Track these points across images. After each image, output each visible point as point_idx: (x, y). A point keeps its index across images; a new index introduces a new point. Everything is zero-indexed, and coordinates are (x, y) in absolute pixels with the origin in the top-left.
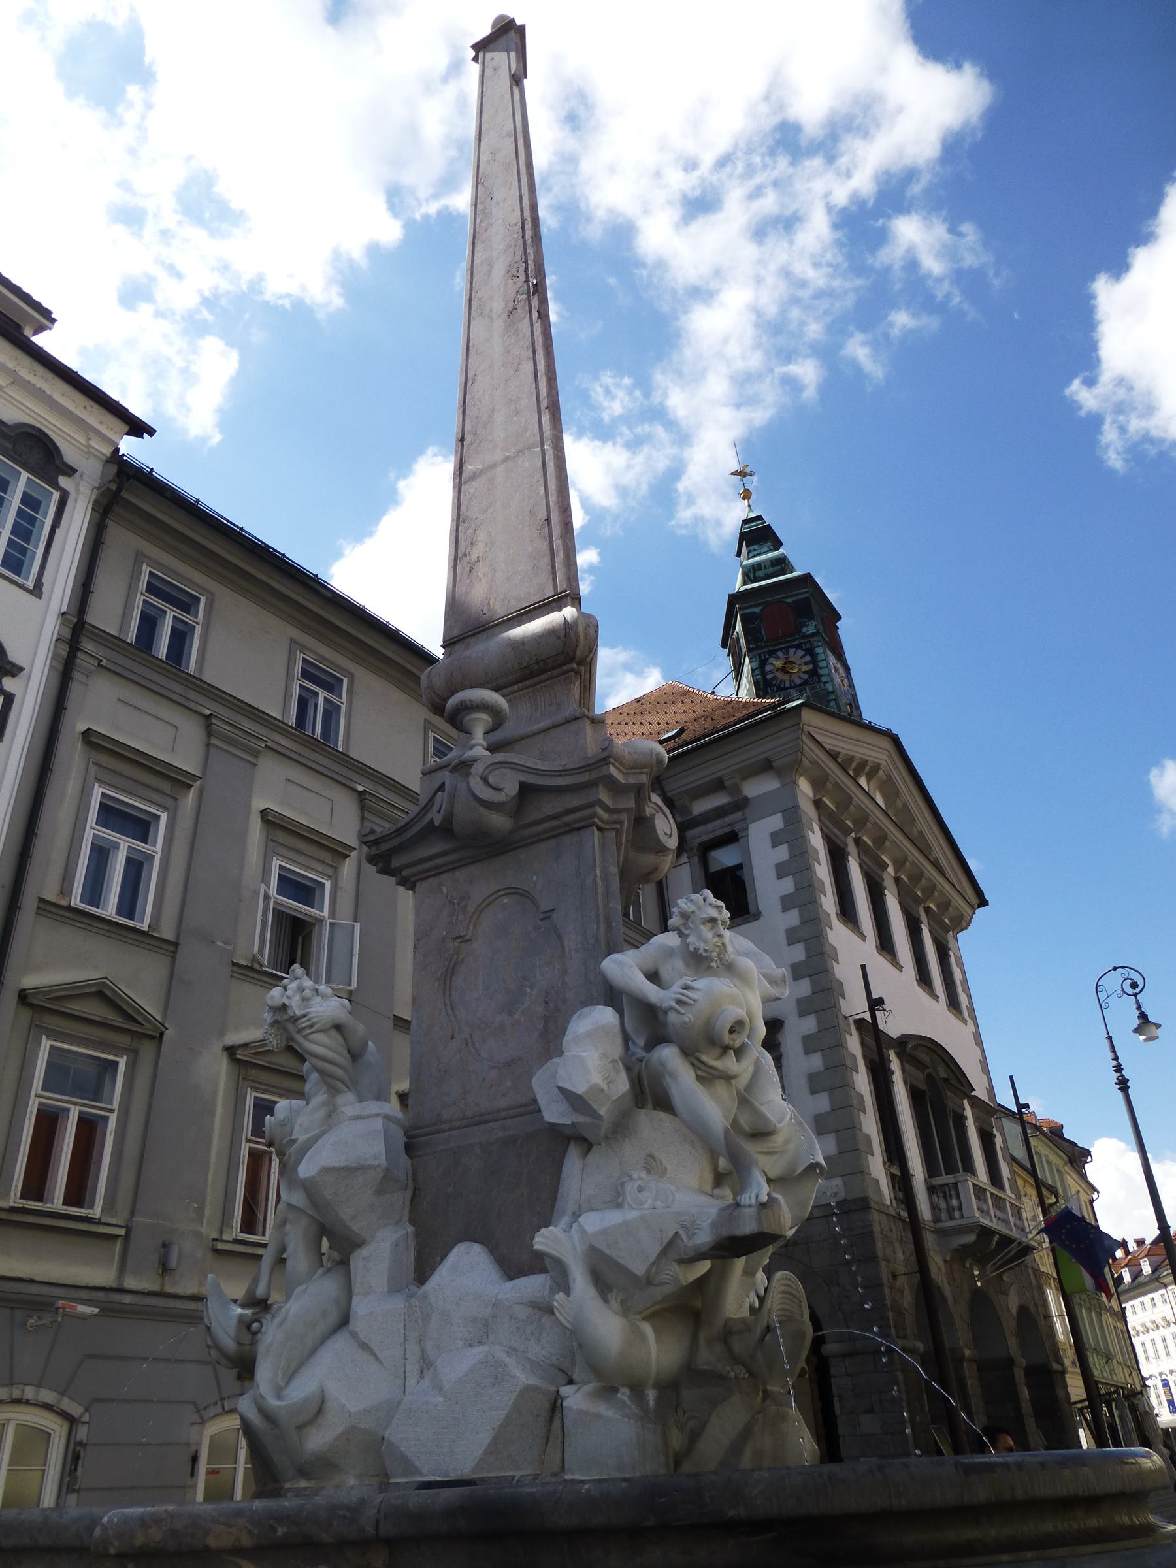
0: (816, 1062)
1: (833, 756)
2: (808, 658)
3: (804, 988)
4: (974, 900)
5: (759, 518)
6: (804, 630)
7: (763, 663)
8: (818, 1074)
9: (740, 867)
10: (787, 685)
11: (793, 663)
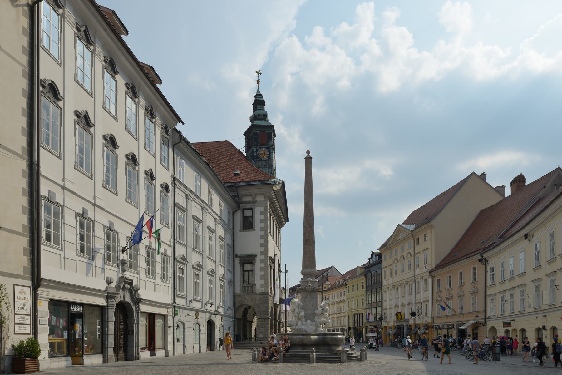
3: (262, 249)
9: (252, 217)
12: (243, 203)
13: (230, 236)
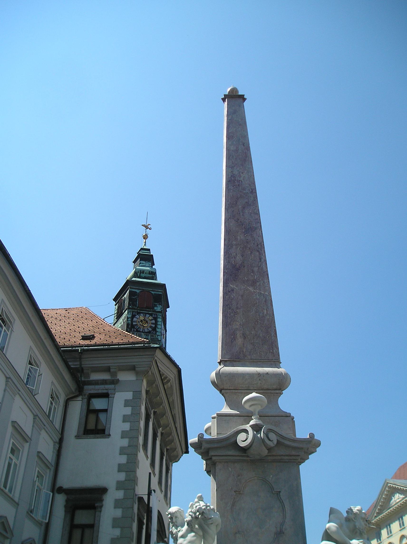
0: (119, 513)
1: (159, 371)
2: (154, 321)
3: (122, 476)
4: (184, 450)
5: (149, 250)
6: (155, 308)
7: (133, 316)
8: (119, 518)
9: (105, 411)
10: (141, 330)
11: (147, 322)
13: (51, 444)
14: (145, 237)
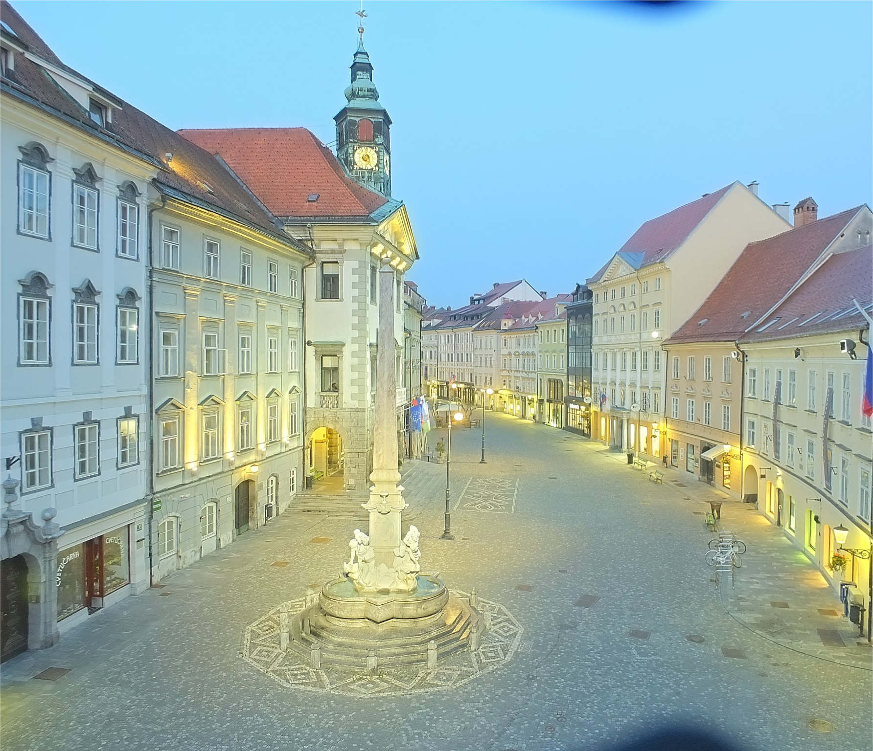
5: (366, 54)
12: (321, 252)
14: (361, 31)
